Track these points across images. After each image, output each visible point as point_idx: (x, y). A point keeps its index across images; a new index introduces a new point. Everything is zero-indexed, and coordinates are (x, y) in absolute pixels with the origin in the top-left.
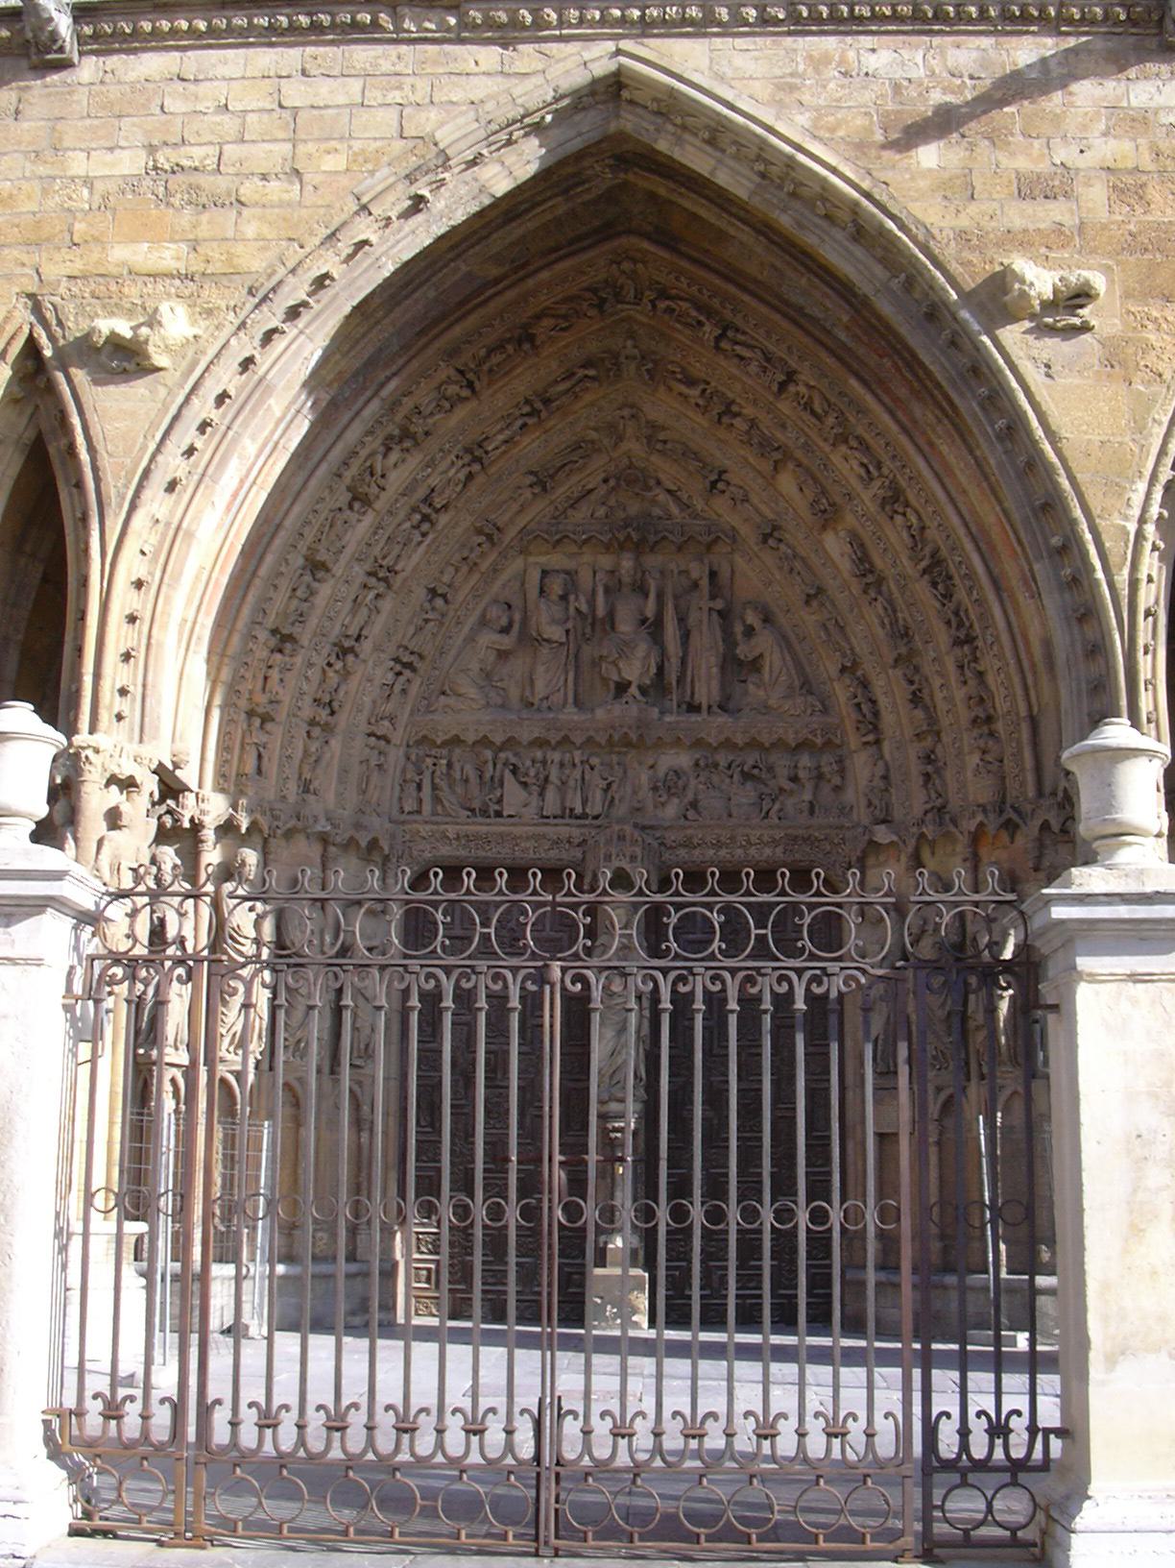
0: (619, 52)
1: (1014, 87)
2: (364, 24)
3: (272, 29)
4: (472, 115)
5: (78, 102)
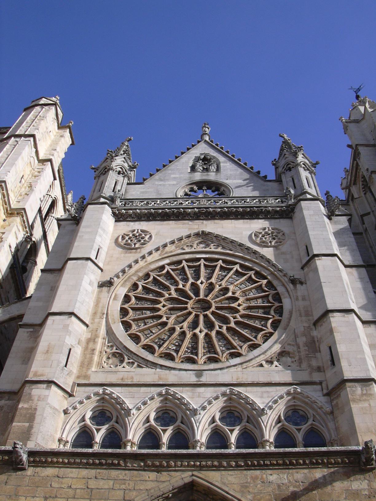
0: (193, 475)
1: (315, 485)
2: (115, 464)
3: (87, 464)
4: (146, 494)
5: (26, 481)
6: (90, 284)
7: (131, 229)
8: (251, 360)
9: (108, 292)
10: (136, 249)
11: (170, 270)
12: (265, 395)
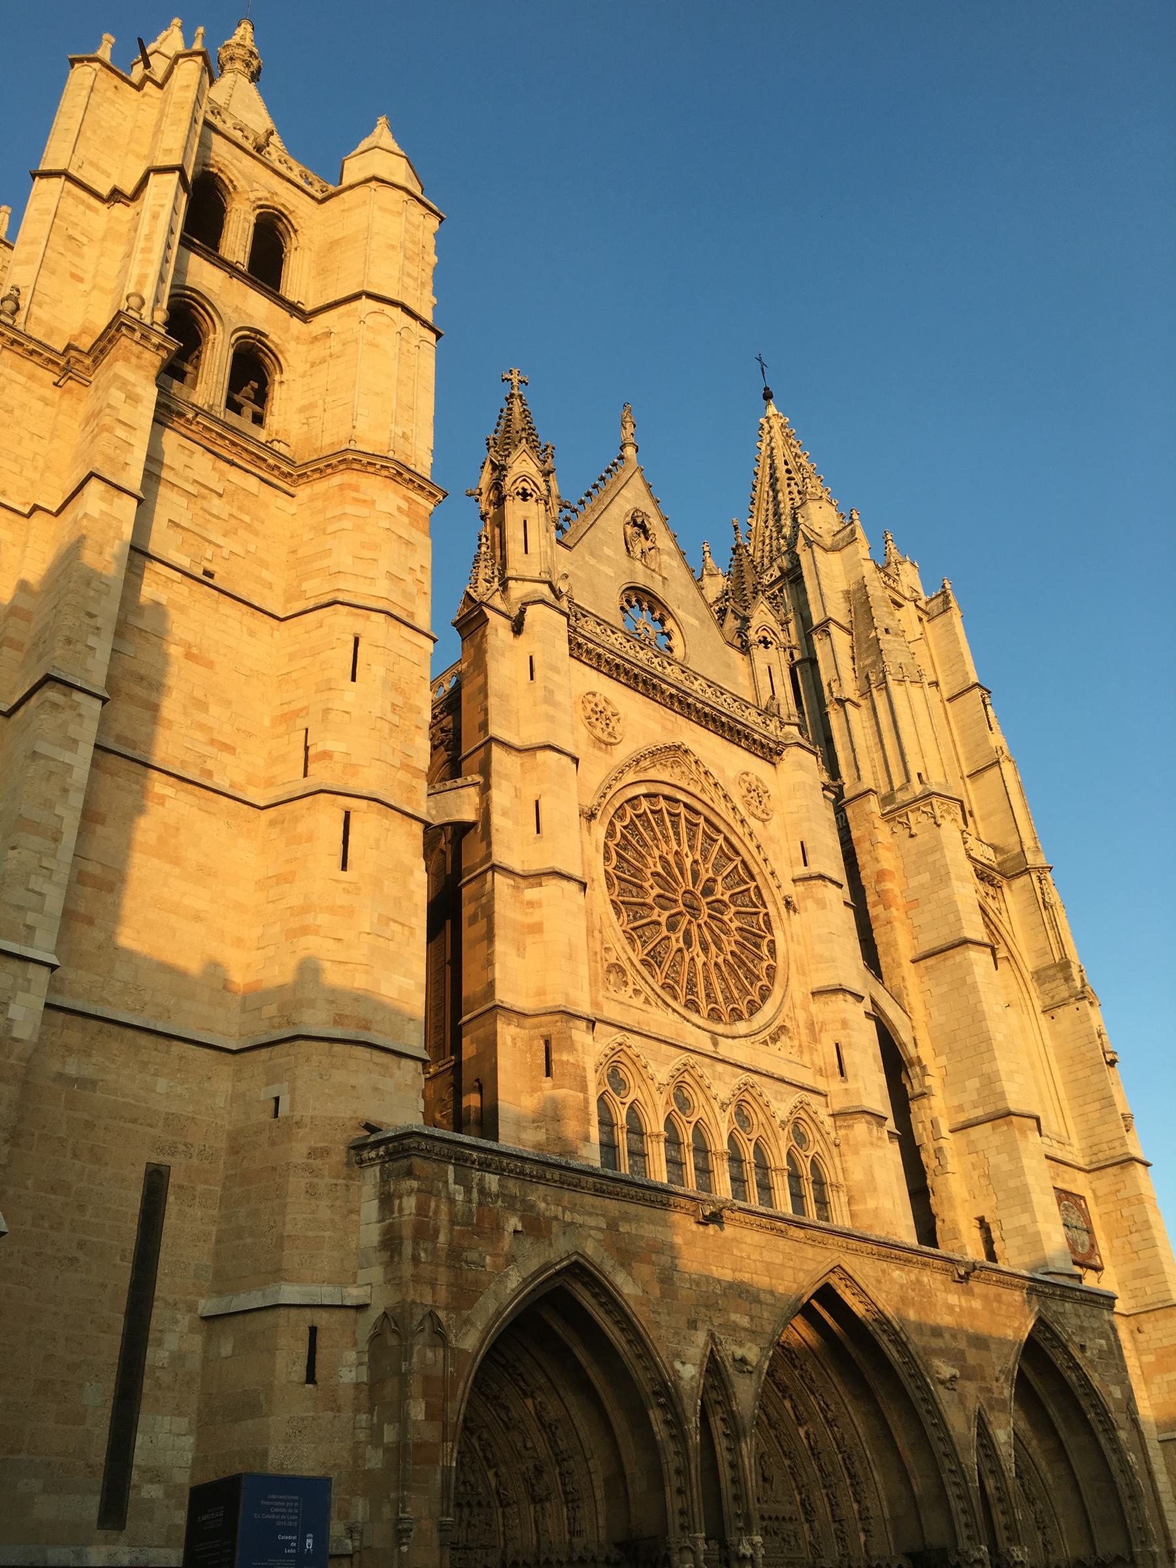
11: (648, 812)
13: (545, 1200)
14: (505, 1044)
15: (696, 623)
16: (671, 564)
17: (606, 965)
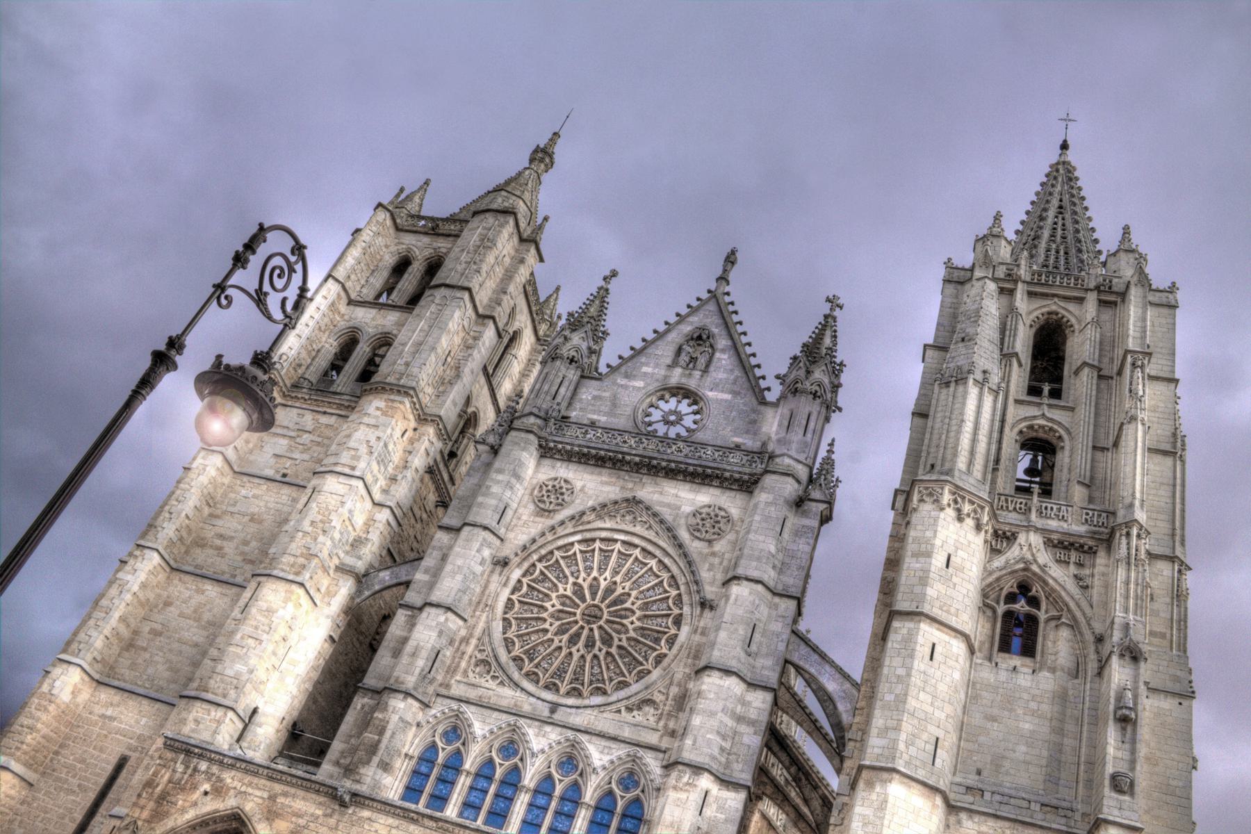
6: (481, 564)
7: (553, 475)
8: (611, 703)
9: (500, 575)
10: (550, 512)
11: (578, 552)
12: (606, 751)
13: (233, 778)
14: (355, 708)
15: (728, 397)
16: (724, 359)
17: (473, 660)
